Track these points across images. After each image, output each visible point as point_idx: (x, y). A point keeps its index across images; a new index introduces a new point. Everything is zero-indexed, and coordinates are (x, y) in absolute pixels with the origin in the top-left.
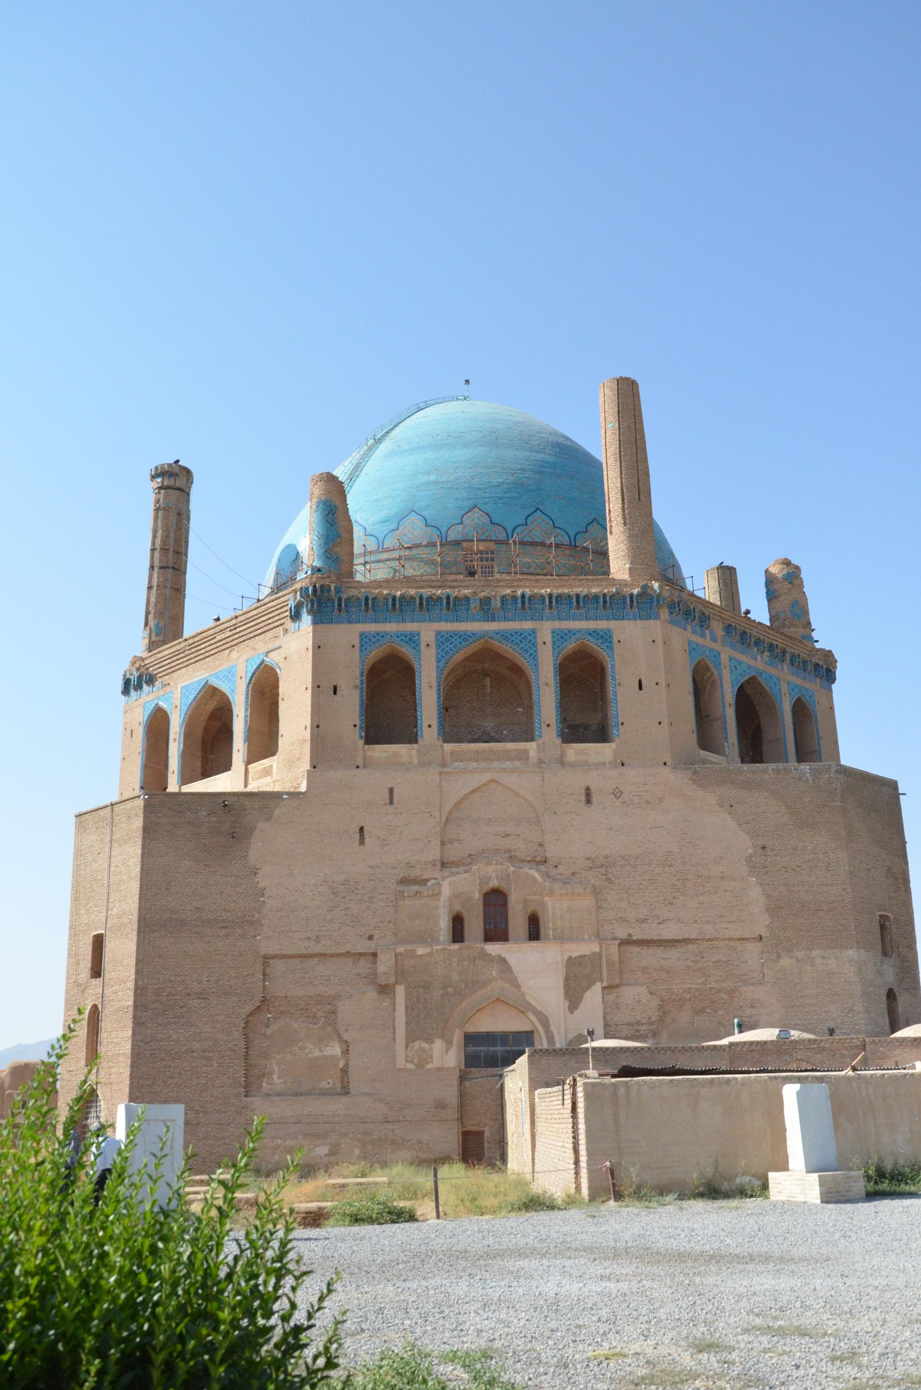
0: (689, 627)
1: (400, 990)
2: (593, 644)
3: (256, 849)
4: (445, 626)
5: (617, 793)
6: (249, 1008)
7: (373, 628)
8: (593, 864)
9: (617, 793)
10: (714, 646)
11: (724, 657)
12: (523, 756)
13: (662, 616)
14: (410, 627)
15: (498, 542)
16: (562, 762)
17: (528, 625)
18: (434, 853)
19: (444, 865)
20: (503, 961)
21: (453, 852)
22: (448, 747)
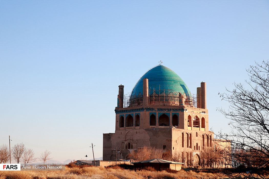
0: (150, 111)
1: (121, 154)
2: (138, 114)
3: (111, 139)
4: (126, 113)
5: (139, 132)
6: (111, 156)
7: (120, 114)
8: (137, 140)
9: (139, 132)
10: (155, 112)
11: (157, 113)
12: (132, 128)
13: (145, 111)
14: (123, 114)
15: (141, 98)
16: (135, 129)
17: (133, 113)
18: (124, 140)
19: (125, 141)
20: (129, 151)
21: (126, 139)
22: (126, 127)
